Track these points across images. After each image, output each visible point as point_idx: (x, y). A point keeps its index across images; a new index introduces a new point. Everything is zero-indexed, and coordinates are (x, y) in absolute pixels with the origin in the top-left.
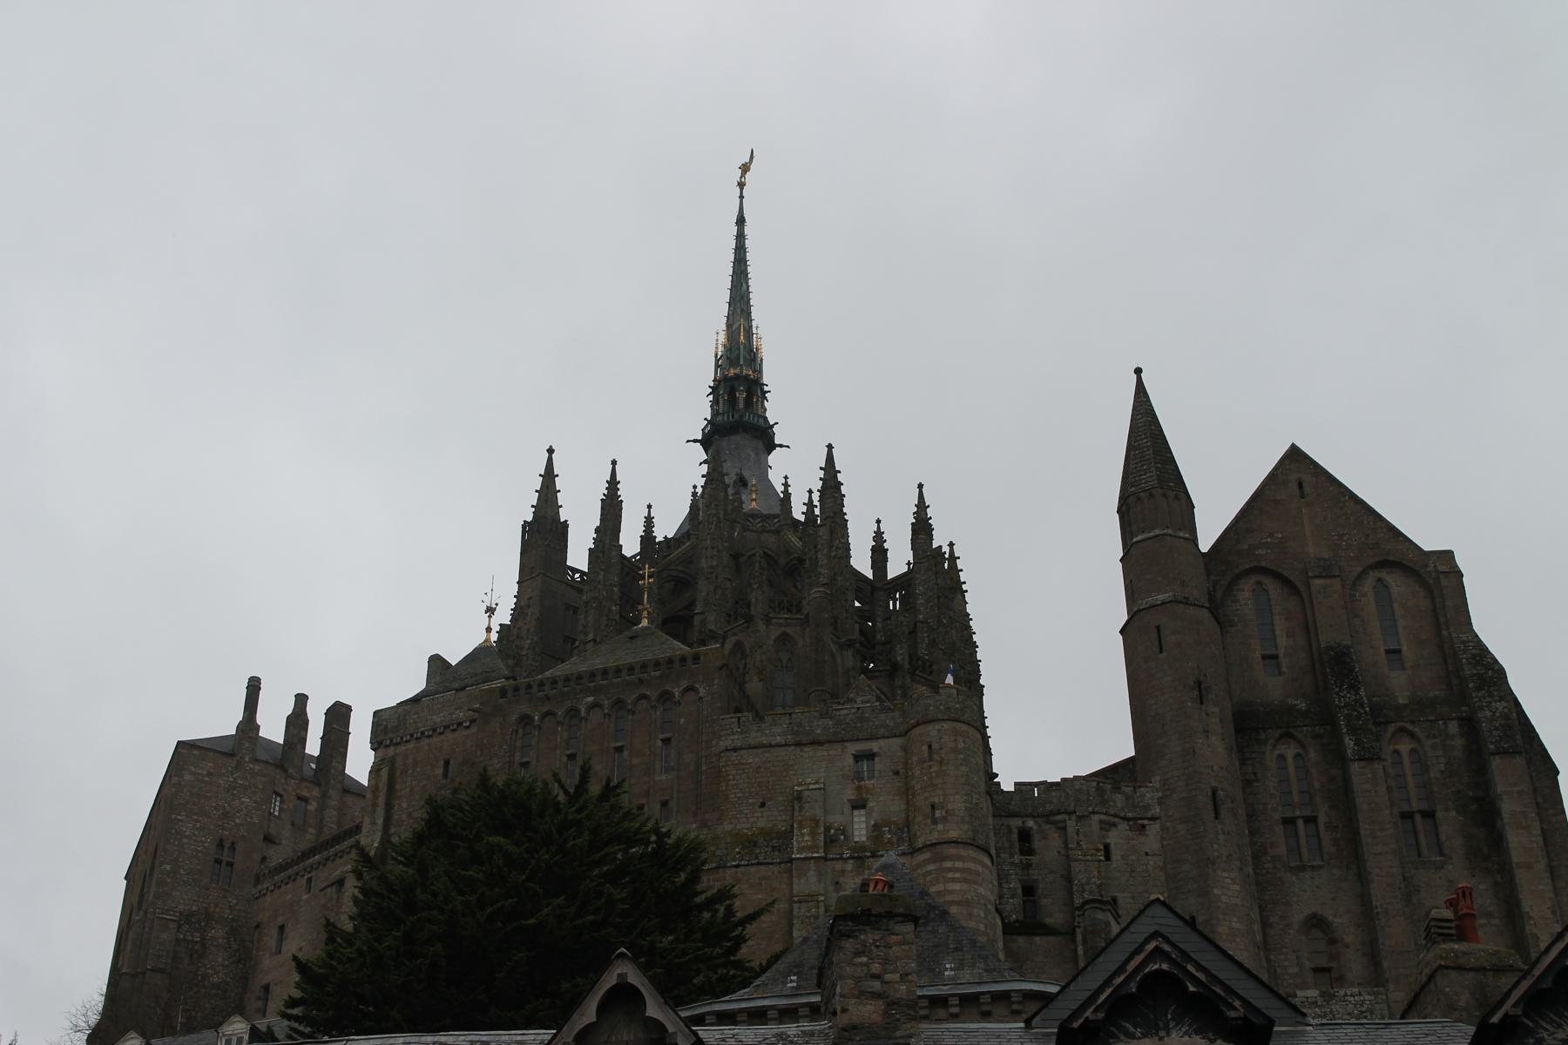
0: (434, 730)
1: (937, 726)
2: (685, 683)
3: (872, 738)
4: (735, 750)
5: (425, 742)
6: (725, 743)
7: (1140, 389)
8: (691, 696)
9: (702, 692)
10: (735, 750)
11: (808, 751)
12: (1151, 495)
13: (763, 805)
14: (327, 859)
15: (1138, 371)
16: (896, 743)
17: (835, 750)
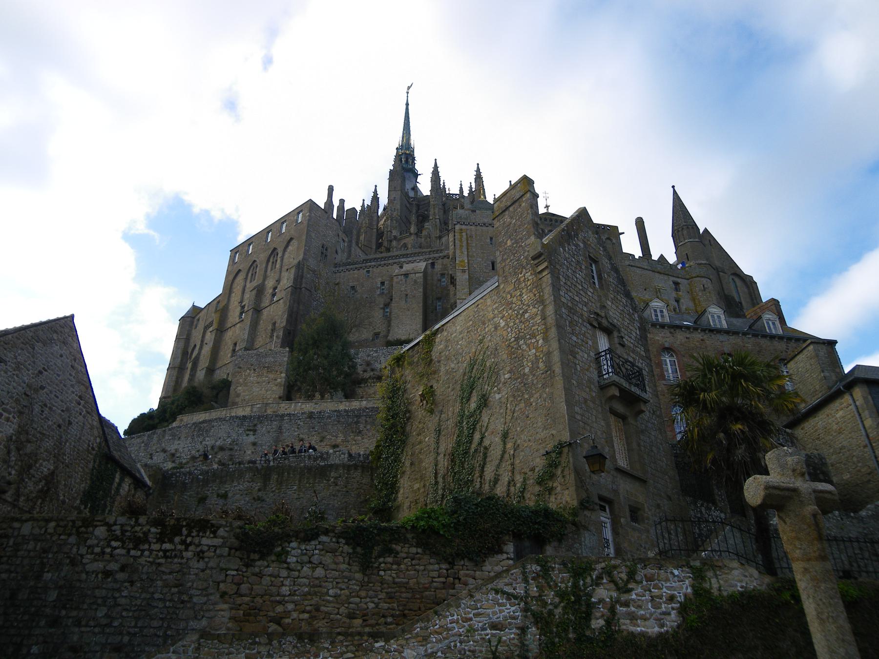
0: (485, 224)
1: (706, 279)
2: (606, 236)
3: (678, 277)
4: (632, 266)
5: (478, 227)
6: (627, 263)
7: (675, 192)
8: (609, 241)
9: (614, 241)
10: (632, 266)
11: (657, 275)
12: (688, 228)
13: (645, 290)
14: (380, 265)
15: (673, 187)
16: (686, 281)
17: (666, 277)
